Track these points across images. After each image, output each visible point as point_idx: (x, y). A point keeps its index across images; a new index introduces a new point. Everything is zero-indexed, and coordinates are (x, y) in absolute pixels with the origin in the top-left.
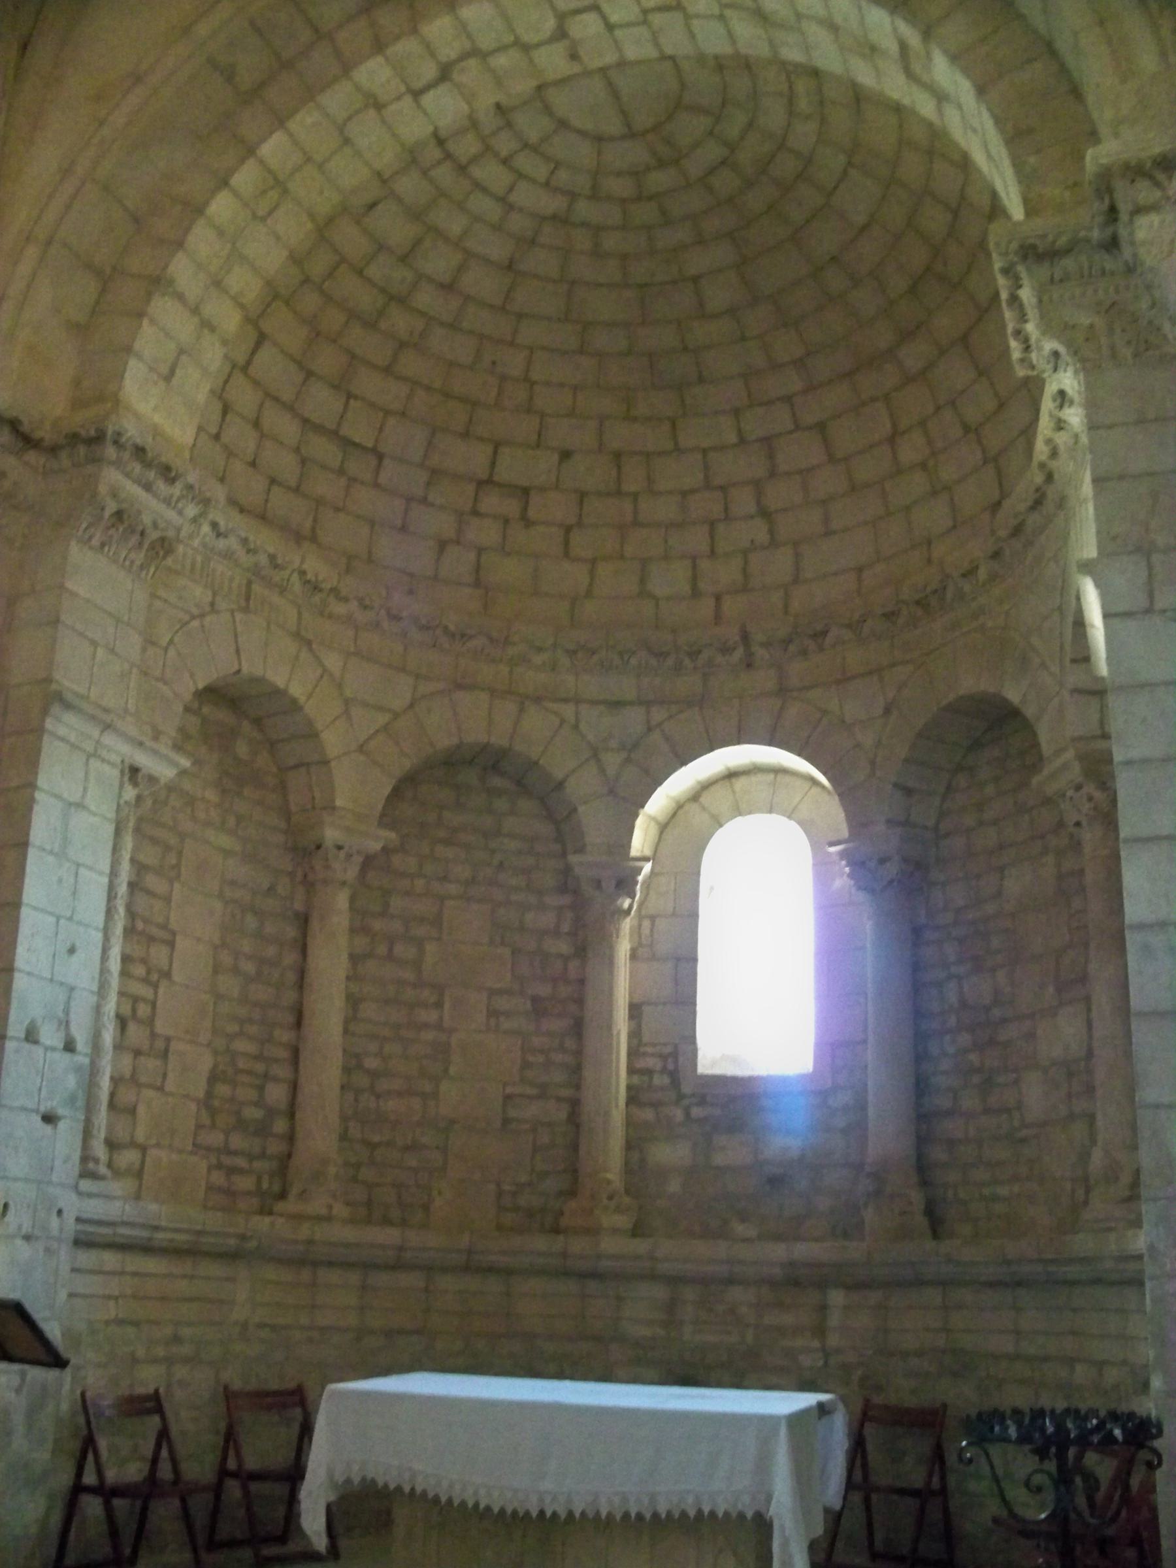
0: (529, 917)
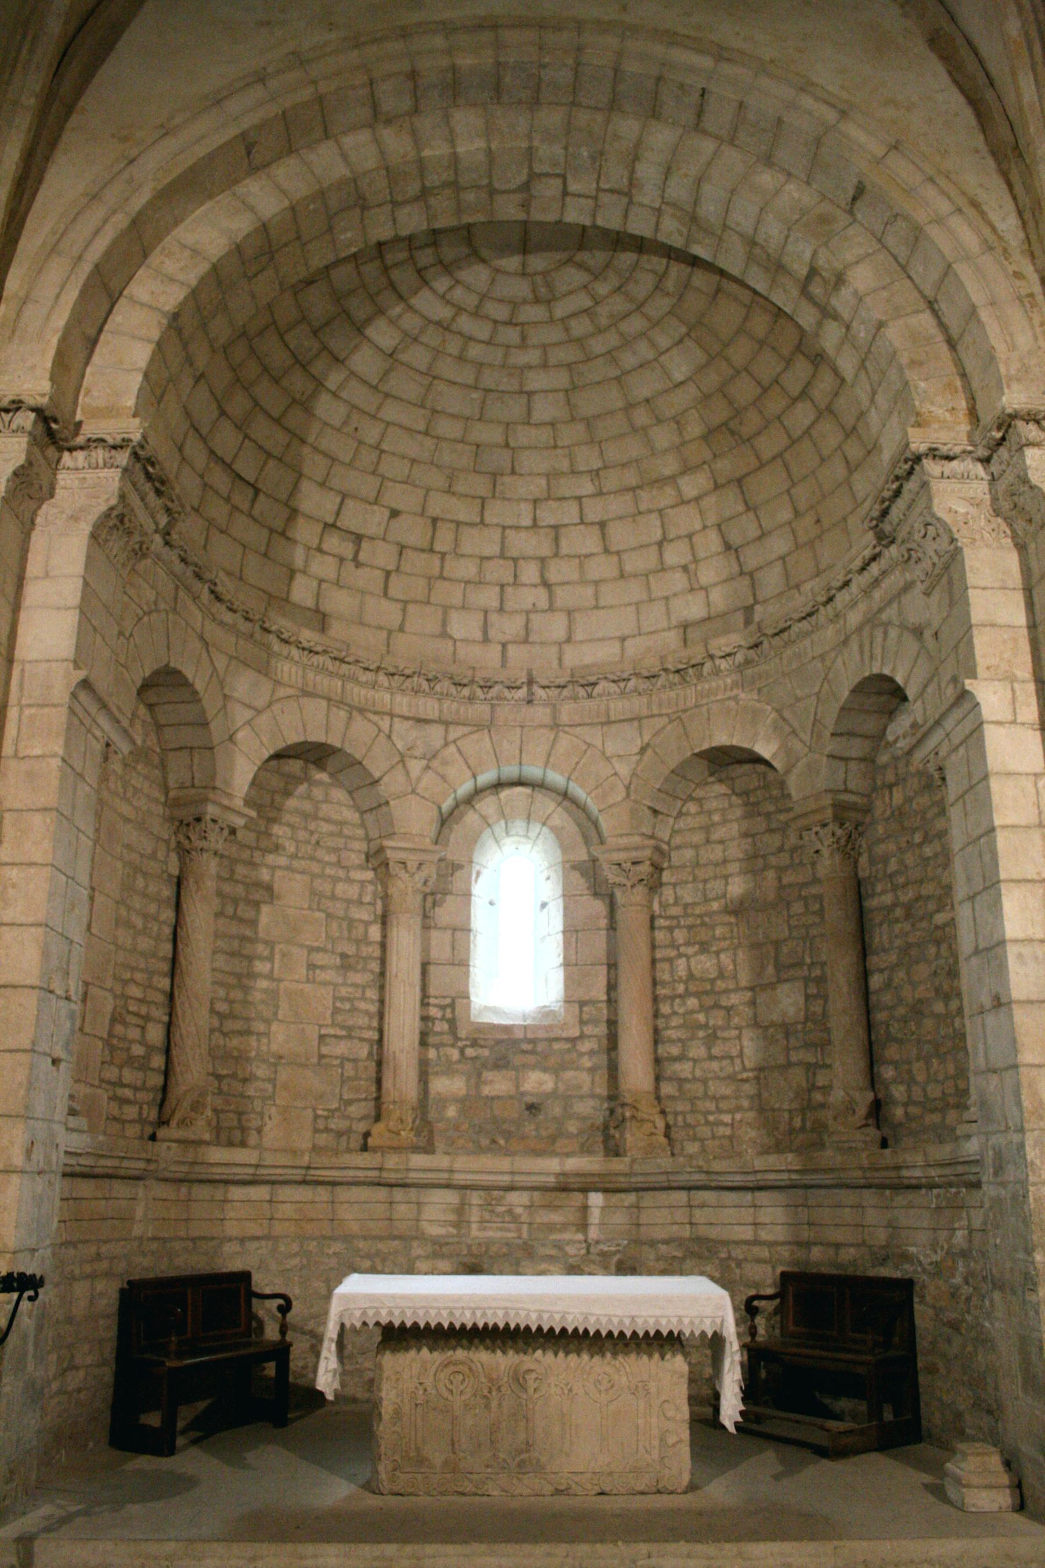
0: (340, 888)
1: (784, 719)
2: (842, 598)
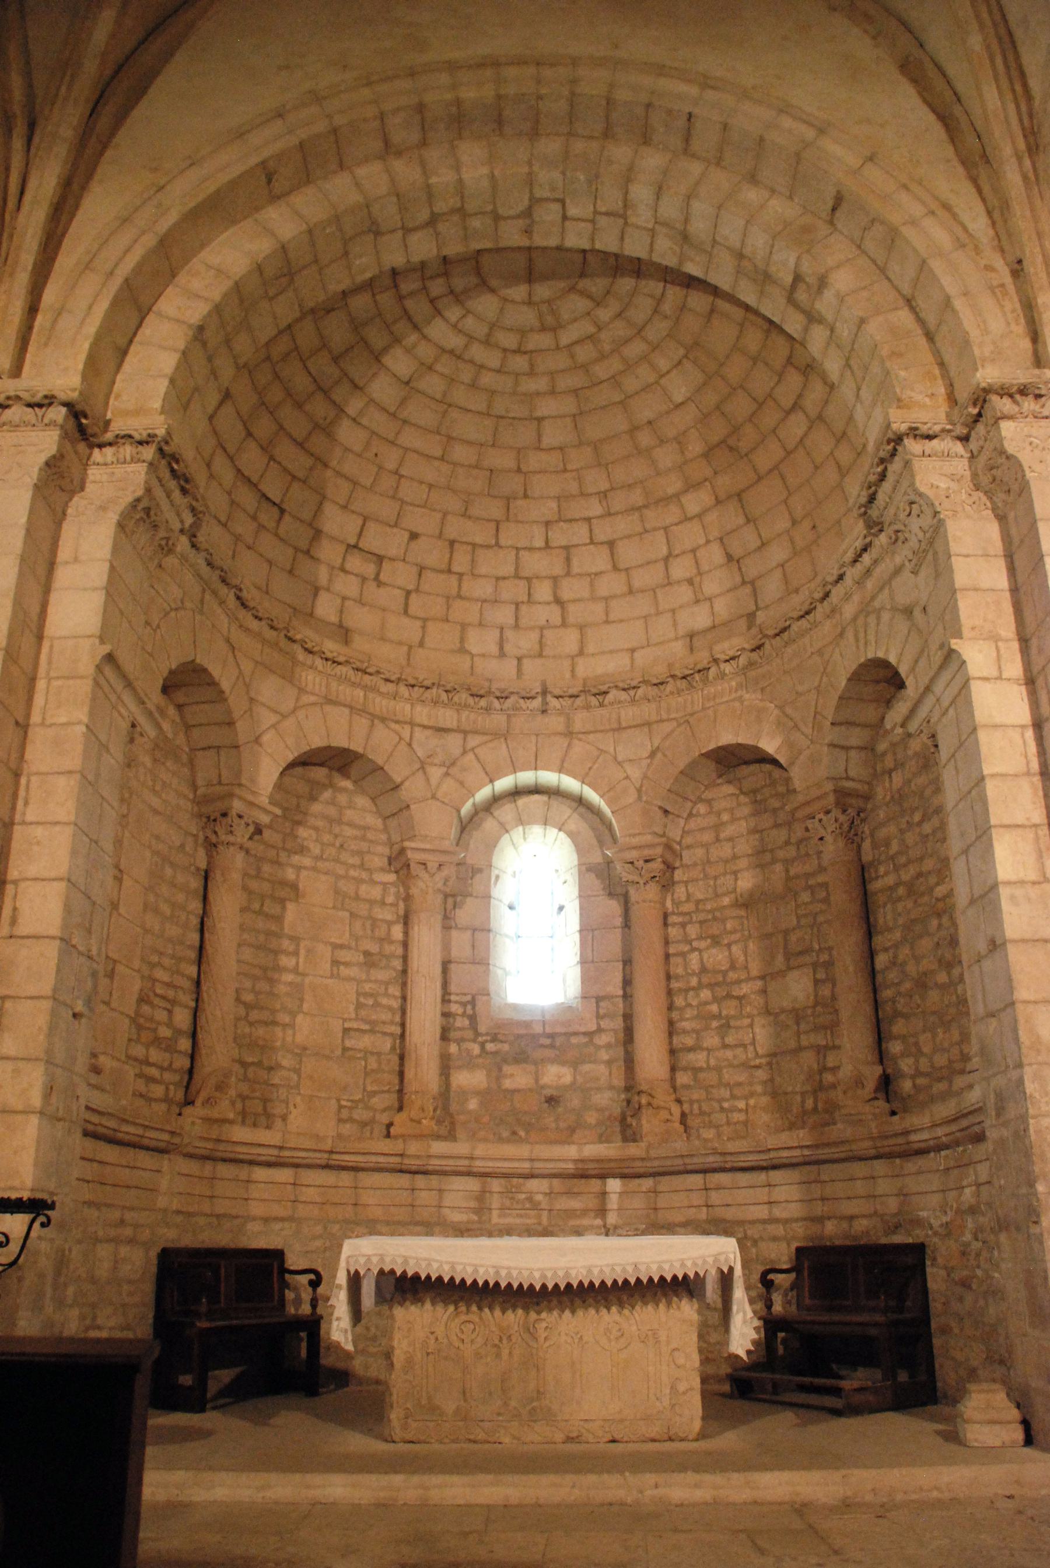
0: (363, 888)
1: (787, 716)
2: (838, 591)
